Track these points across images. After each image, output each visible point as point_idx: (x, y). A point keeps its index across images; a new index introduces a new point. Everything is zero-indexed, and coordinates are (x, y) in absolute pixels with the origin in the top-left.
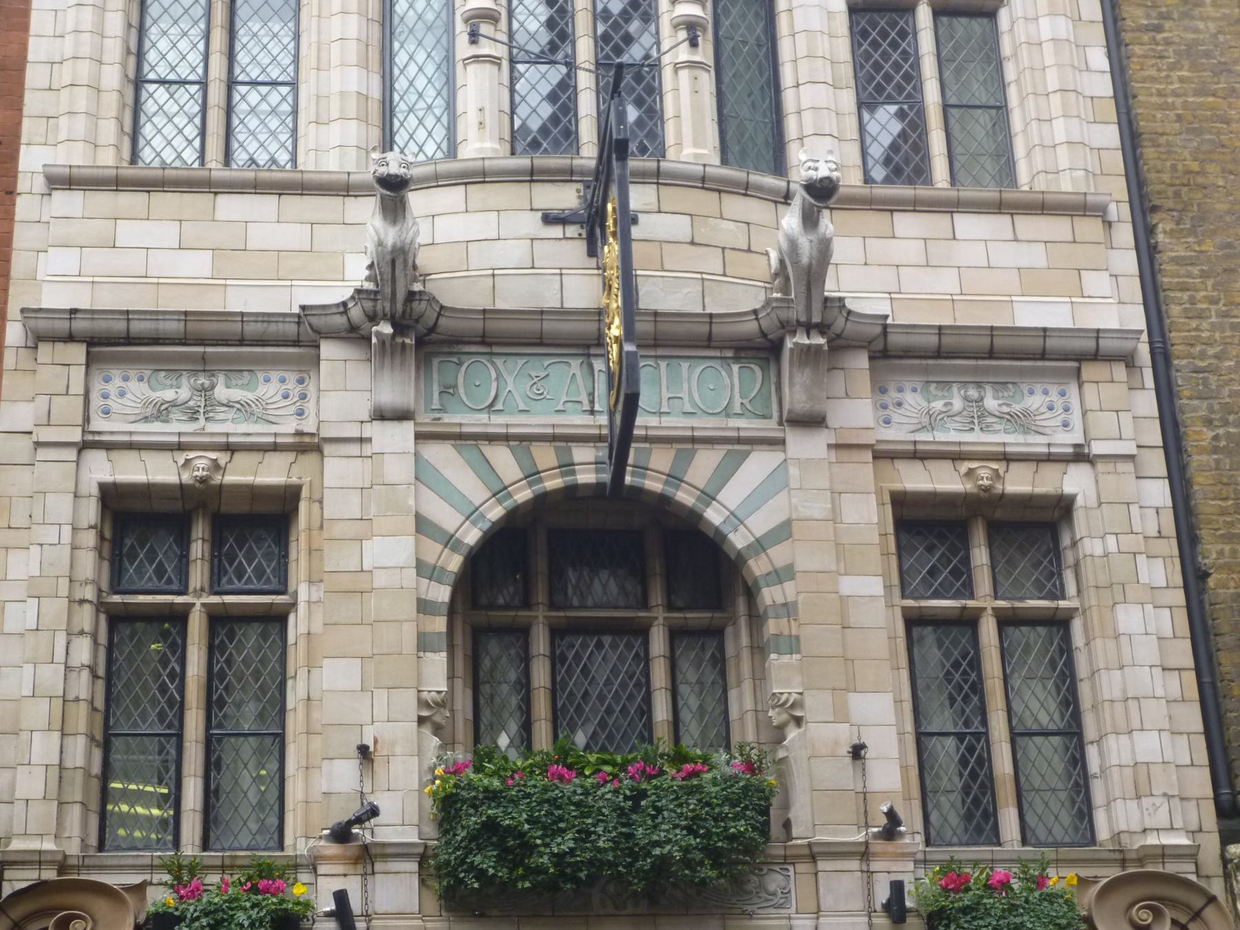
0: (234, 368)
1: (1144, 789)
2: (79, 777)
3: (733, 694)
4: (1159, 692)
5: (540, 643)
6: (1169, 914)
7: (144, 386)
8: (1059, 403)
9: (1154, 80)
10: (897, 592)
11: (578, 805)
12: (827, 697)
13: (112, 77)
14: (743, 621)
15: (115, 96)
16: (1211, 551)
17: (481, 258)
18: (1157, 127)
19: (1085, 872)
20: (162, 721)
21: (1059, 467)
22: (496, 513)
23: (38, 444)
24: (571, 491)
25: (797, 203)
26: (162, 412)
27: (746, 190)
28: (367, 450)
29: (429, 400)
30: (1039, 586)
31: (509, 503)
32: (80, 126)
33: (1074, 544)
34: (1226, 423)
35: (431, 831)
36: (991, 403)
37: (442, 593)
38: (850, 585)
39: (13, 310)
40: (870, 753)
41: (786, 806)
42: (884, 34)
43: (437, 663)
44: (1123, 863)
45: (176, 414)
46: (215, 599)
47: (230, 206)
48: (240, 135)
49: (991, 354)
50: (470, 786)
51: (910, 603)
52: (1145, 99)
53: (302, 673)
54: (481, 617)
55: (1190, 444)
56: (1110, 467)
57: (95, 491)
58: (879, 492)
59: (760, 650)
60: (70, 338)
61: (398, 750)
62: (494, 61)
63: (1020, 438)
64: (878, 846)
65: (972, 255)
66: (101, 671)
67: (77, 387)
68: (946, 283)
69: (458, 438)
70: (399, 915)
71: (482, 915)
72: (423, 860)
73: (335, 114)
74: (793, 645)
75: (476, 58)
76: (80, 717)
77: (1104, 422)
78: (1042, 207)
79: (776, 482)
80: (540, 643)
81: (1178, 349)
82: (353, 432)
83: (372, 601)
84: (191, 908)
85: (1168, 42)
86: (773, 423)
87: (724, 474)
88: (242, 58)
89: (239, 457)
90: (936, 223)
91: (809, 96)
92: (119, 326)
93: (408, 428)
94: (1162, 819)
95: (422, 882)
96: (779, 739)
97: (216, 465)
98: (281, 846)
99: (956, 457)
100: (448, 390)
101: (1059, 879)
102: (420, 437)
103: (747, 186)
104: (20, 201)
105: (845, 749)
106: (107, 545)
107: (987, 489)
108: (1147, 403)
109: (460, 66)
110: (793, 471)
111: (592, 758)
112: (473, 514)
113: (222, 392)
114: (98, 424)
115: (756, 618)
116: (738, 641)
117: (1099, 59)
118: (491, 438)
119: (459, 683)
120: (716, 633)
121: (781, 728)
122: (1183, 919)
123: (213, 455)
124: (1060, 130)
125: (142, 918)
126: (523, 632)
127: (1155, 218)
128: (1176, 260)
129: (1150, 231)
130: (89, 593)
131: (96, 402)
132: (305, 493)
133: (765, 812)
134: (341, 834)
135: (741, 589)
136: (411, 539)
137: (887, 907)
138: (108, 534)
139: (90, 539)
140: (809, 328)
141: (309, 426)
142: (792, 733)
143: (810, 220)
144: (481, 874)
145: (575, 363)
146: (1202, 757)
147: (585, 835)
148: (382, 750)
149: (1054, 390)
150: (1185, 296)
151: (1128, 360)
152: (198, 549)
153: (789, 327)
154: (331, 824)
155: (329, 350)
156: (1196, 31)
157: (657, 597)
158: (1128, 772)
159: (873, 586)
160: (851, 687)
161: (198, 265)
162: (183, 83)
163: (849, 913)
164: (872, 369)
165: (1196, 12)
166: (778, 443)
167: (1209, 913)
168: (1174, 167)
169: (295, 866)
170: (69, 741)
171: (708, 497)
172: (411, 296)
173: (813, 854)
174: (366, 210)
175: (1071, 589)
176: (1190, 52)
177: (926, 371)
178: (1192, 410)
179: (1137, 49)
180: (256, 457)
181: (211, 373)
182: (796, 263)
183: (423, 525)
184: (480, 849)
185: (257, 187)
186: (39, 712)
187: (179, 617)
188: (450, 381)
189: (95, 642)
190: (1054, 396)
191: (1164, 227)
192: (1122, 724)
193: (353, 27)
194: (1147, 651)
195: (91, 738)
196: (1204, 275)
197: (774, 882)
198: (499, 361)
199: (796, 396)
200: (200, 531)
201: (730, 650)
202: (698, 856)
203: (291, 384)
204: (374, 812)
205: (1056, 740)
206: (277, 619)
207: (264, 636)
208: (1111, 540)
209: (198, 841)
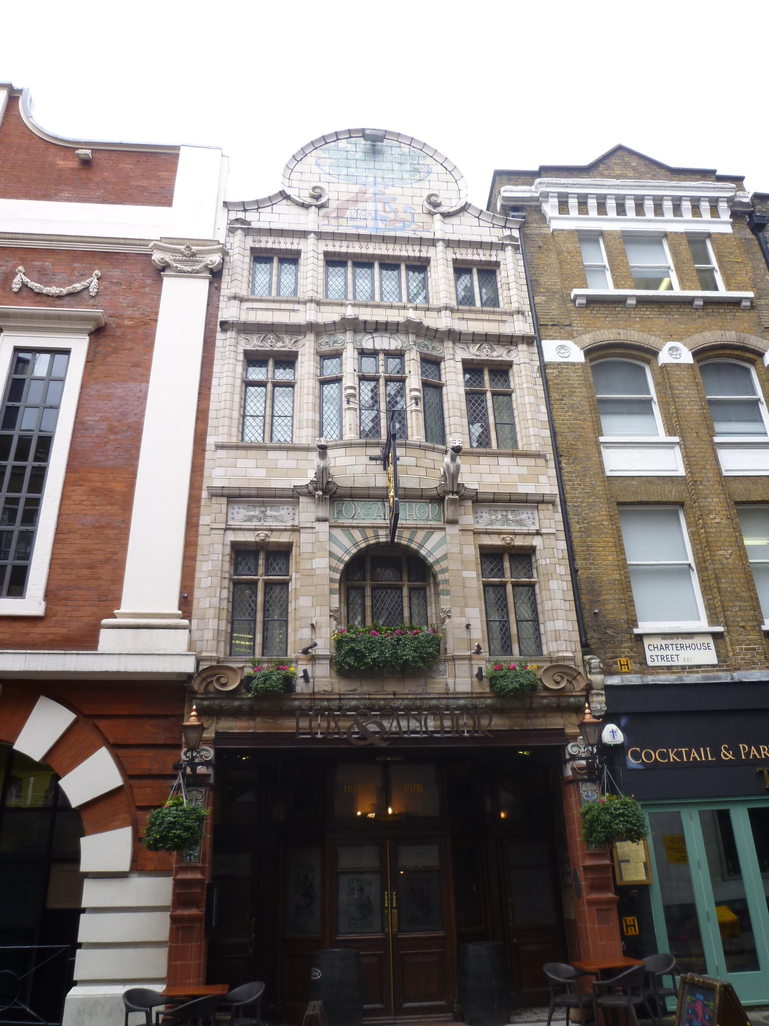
0: (274, 505)
1: (558, 638)
2: (224, 633)
3: (429, 608)
4: (563, 608)
5: (368, 592)
6: (566, 678)
7: (245, 510)
8: (531, 516)
9: (560, 415)
10: (481, 576)
11: (380, 643)
12: (458, 609)
13: (236, 414)
14: (432, 585)
15: (237, 420)
16: (579, 563)
17: (350, 471)
18: (562, 430)
19: (539, 665)
20: (249, 615)
21: (532, 537)
22: (354, 551)
23: (212, 529)
24: (378, 544)
25: (449, 453)
26: (250, 519)
27: (433, 449)
28: (314, 531)
29: (333, 515)
30: (525, 574)
31: (358, 548)
32: (226, 429)
33: (536, 561)
34: (584, 523)
35: (334, 651)
36: (510, 517)
37: (337, 576)
38: (466, 574)
39: (204, 487)
40: (472, 627)
41: (445, 644)
42: (476, 401)
43: (335, 598)
44: (551, 661)
45: (254, 520)
46: (266, 578)
47: (272, 455)
48: (275, 432)
49: (510, 501)
50: (346, 637)
51: (485, 579)
52: (558, 422)
53: (293, 601)
55: (572, 530)
56: (547, 537)
57: (229, 543)
58: (475, 545)
59: (437, 594)
60: (222, 496)
61: (323, 625)
62: (355, 409)
63: (519, 528)
64: (475, 656)
65: (505, 470)
66: (231, 600)
67: (224, 511)
68: (496, 479)
69: (343, 527)
70: (323, 677)
71: (349, 677)
72: (331, 660)
73: (305, 426)
74: (448, 593)
75: (349, 409)
76: (224, 614)
77: (546, 522)
78: (526, 455)
79: (443, 541)
80: (368, 592)
81: (568, 500)
82: (310, 525)
83: (315, 578)
84: (258, 675)
85: (565, 404)
86: (442, 523)
87: (426, 539)
88: (276, 408)
89: (274, 533)
90: (493, 460)
91: (453, 420)
92: (237, 492)
93: (327, 524)
94: (564, 648)
95: (331, 667)
96: (443, 621)
97: (267, 536)
98: (287, 655)
99: (499, 533)
100: (340, 512)
101: (531, 666)
102: (330, 527)
103: (434, 448)
104: (207, 453)
105: (464, 626)
106: (233, 561)
107: (509, 544)
108: (559, 516)
109: (344, 411)
110: (448, 538)
111: (384, 628)
112: (347, 551)
113: (269, 513)
114: (230, 523)
115: (436, 584)
116: (431, 591)
117: (543, 409)
118: (353, 527)
119: (342, 604)
120: (424, 589)
121: (444, 619)
122: (570, 679)
123: (266, 532)
124: (531, 431)
125: (243, 677)
126: (363, 588)
127: (561, 459)
128: (568, 472)
129: (560, 463)
130: (227, 575)
131: (230, 515)
132: (294, 544)
133: (439, 645)
134: (305, 652)
135: (431, 575)
136: (327, 560)
137: (477, 675)
138: (233, 557)
139: (227, 558)
140: (453, 493)
141: (296, 523)
142: (447, 621)
143: (453, 459)
144: (349, 665)
145: (380, 504)
146: (576, 628)
147: (382, 652)
148: (318, 626)
149: (530, 512)
150: (571, 483)
151: (553, 503)
152: (261, 562)
153: (446, 493)
154: (303, 648)
155: (302, 499)
156: (574, 400)
157: (405, 577)
158: (553, 633)
159: (473, 574)
160: (466, 606)
161: (261, 473)
162: (258, 416)
163: (465, 677)
164: (473, 506)
165: (574, 394)
166: (444, 529)
167: (579, 677)
168: (567, 443)
169: (291, 661)
170: (221, 621)
171: (421, 546)
172: (328, 483)
173: (454, 659)
174: (314, 456)
175: (535, 575)
176: (572, 407)
177: (490, 506)
178: (573, 519)
179: (555, 406)
180: (280, 533)
181: (266, 507)
182: (449, 472)
183: (331, 555)
184: (349, 656)
185: (280, 449)
186: (211, 613)
187: (255, 583)
188: (340, 509)
189: (229, 591)
190: (530, 515)
191: (564, 461)
192: (551, 617)
193: (311, 399)
194: (559, 595)
195: (228, 621)
196: (577, 477)
197: (442, 667)
198: (355, 503)
199: (449, 513)
200: (262, 556)
201: (428, 594)
202: (417, 659)
204: (315, 645)
205: (530, 623)
206: (285, 584)
207: (282, 589)
208: (548, 560)
209: (260, 653)
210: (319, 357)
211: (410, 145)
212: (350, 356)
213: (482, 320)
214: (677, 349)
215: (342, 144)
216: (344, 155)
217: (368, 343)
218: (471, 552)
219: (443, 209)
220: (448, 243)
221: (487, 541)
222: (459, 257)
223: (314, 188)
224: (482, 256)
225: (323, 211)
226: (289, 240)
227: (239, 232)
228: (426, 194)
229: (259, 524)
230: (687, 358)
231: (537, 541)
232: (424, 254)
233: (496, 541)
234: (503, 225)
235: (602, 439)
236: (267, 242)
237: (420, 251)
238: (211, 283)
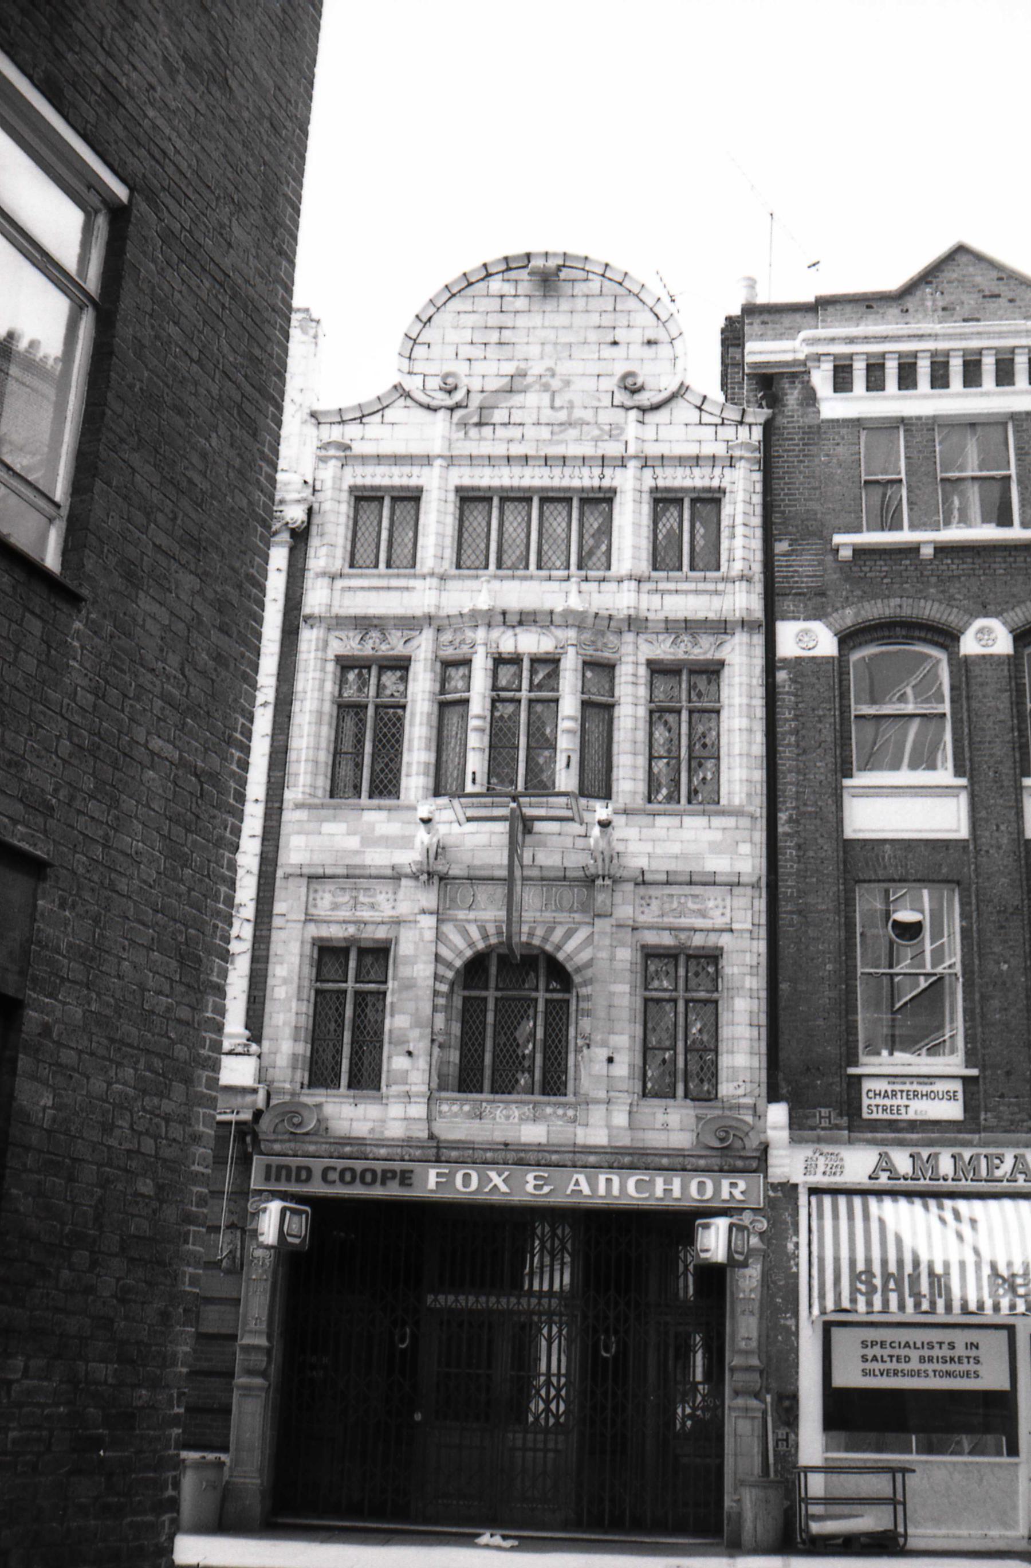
54: (467, 993)
60: (301, 875)
67: (304, 898)
68: (676, 849)
74: (588, 1013)
79: (589, 940)
82: (411, 918)
100: (453, 900)
110: (596, 937)
112: (460, 953)
114: (312, 911)
139: (307, 961)
146: (764, 1064)
152: (352, 964)
155: (404, 882)
159: (626, 988)
160: (611, 1032)
161: (353, 843)
171: (559, 948)
183: (438, 958)
186: (287, 1032)
203: (390, 896)
210: (438, 665)
211: (603, 275)
212: (481, 666)
213: (686, 592)
214: (990, 631)
215: (496, 285)
216: (494, 304)
217: (508, 642)
218: (625, 955)
219: (645, 399)
220: (646, 462)
221: (651, 938)
222: (661, 483)
223: (447, 375)
224: (698, 479)
225: (459, 414)
226: (406, 470)
227: (333, 463)
228: (620, 369)
229: (348, 914)
230: (1003, 644)
231: (725, 940)
232: (606, 483)
233: (667, 940)
234: (739, 418)
235: (847, 782)
236: (373, 476)
237: (602, 477)
238: (292, 550)
